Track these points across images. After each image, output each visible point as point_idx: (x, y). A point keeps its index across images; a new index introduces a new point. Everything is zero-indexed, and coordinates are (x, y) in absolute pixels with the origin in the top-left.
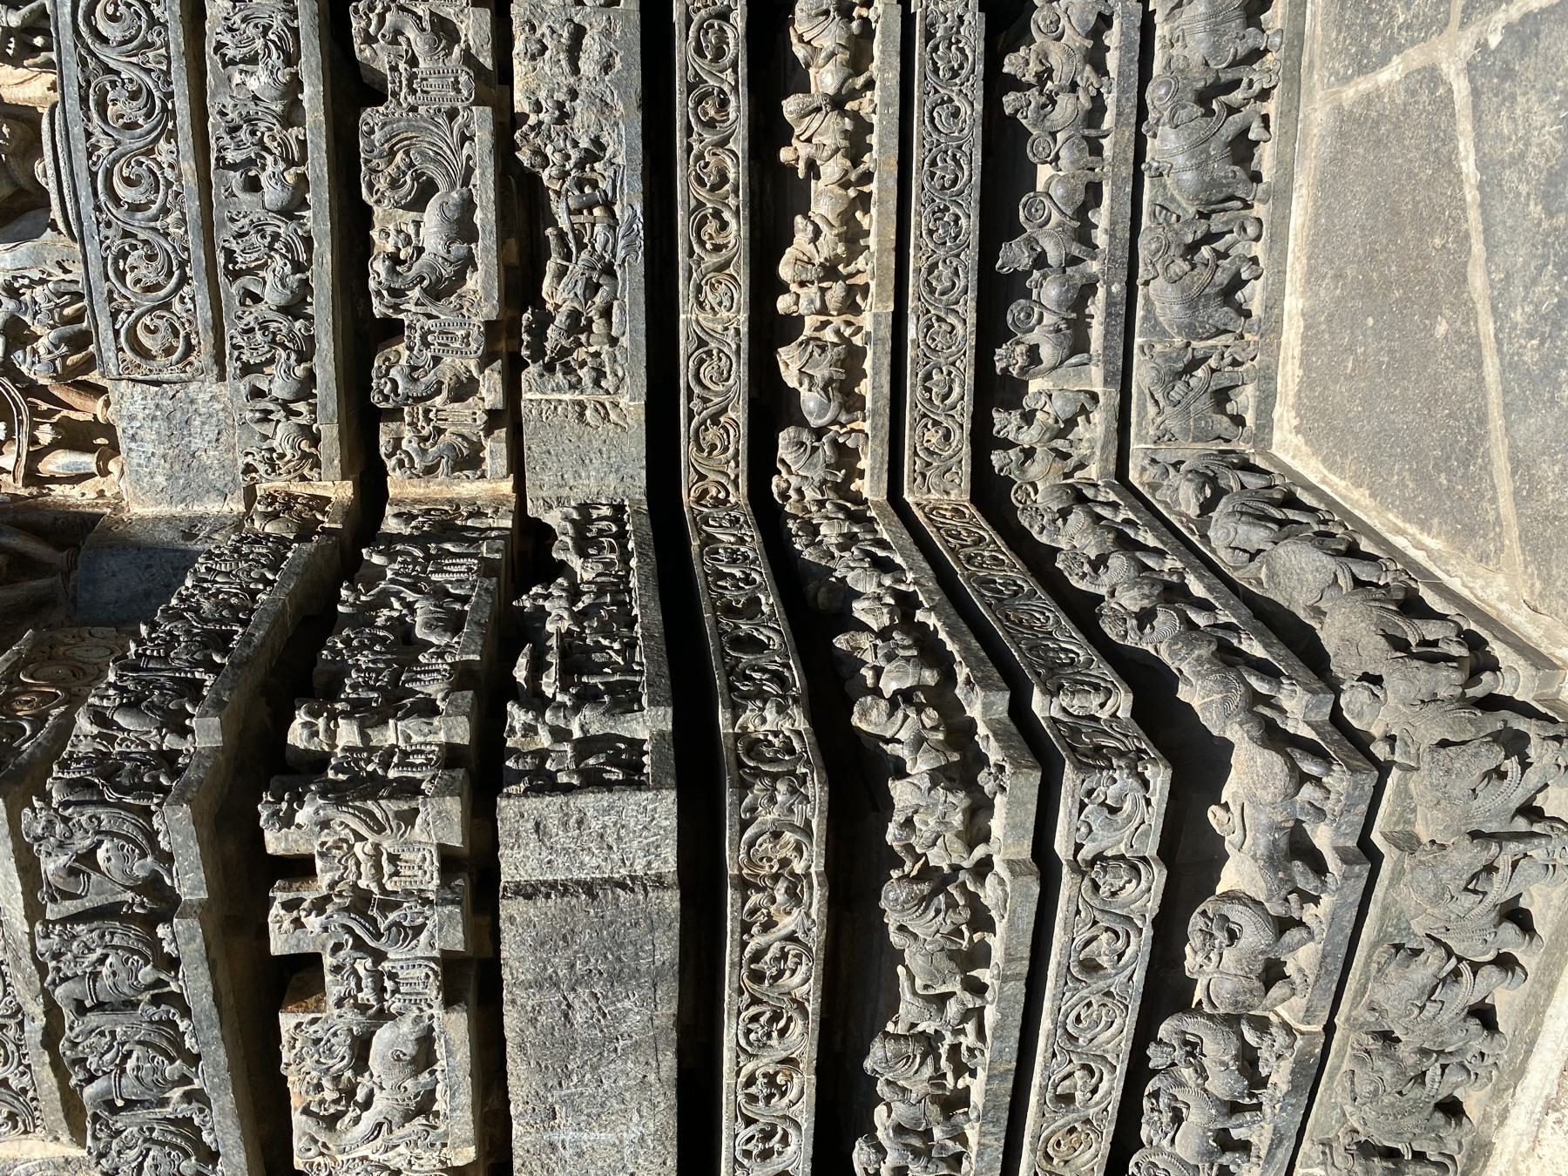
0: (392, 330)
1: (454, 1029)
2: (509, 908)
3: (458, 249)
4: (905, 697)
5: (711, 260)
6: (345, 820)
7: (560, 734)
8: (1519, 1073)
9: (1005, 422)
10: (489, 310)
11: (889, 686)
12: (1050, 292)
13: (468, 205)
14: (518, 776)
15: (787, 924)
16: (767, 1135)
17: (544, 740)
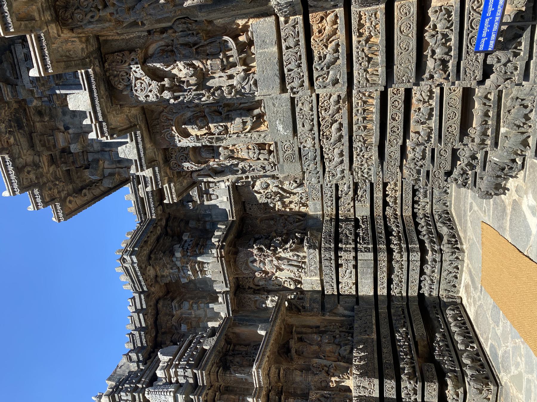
0: (341, 197)
1: (354, 271)
2: (358, 261)
3: (349, 190)
4: (396, 244)
5: (378, 189)
6: (345, 254)
7: (362, 247)
8: (461, 283)
9: (416, 206)
10: (352, 196)
11: (395, 243)
12: (422, 191)
13: (350, 185)
14: (359, 251)
15: (383, 264)
16: (382, 283)
17: (361, 247)
